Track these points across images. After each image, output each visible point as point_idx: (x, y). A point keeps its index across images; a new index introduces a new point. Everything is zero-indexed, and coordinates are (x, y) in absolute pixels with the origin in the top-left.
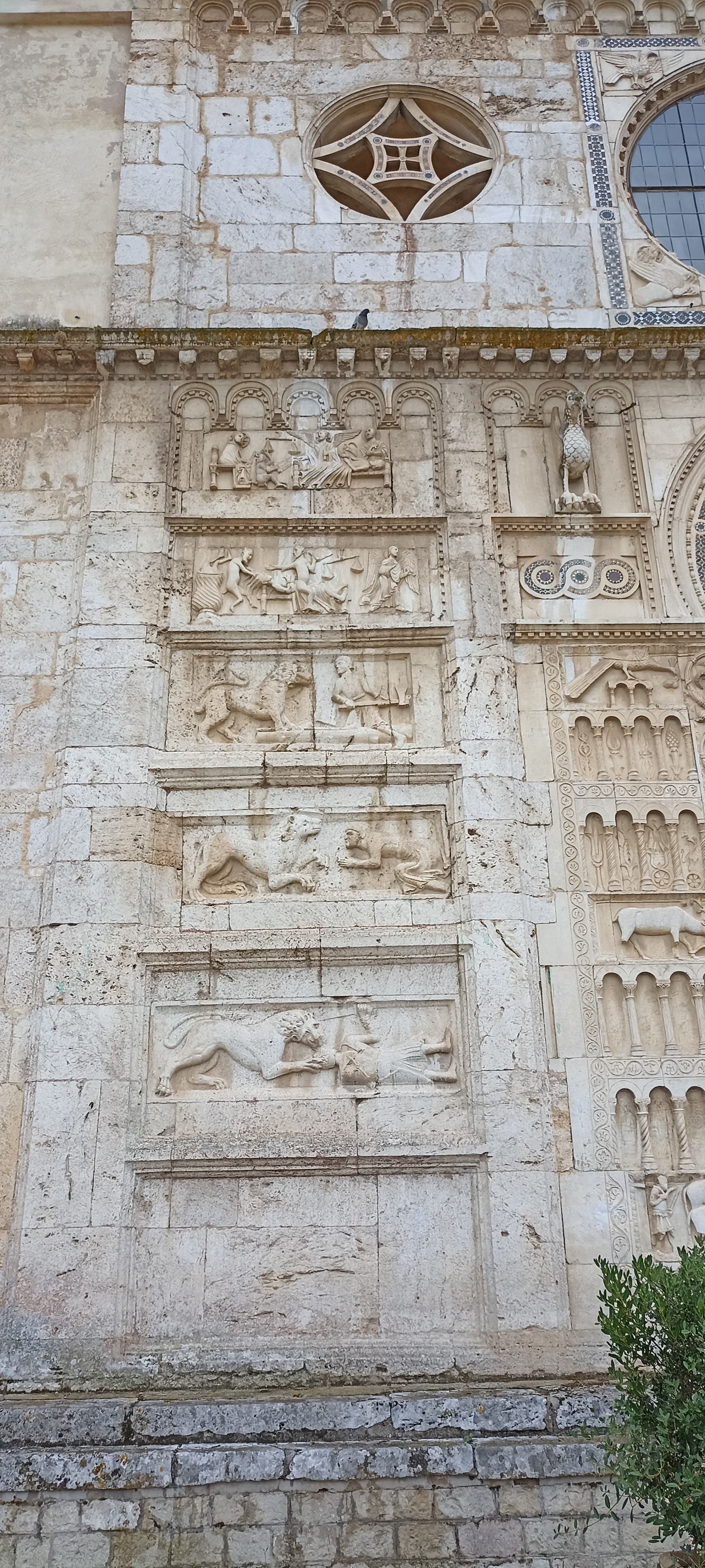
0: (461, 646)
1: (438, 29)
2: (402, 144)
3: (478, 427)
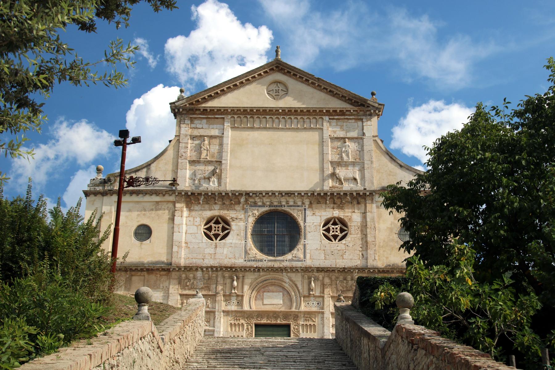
0: (216, 313)
1: (224, 204)
2: (217, 226)
3: (222, 280)
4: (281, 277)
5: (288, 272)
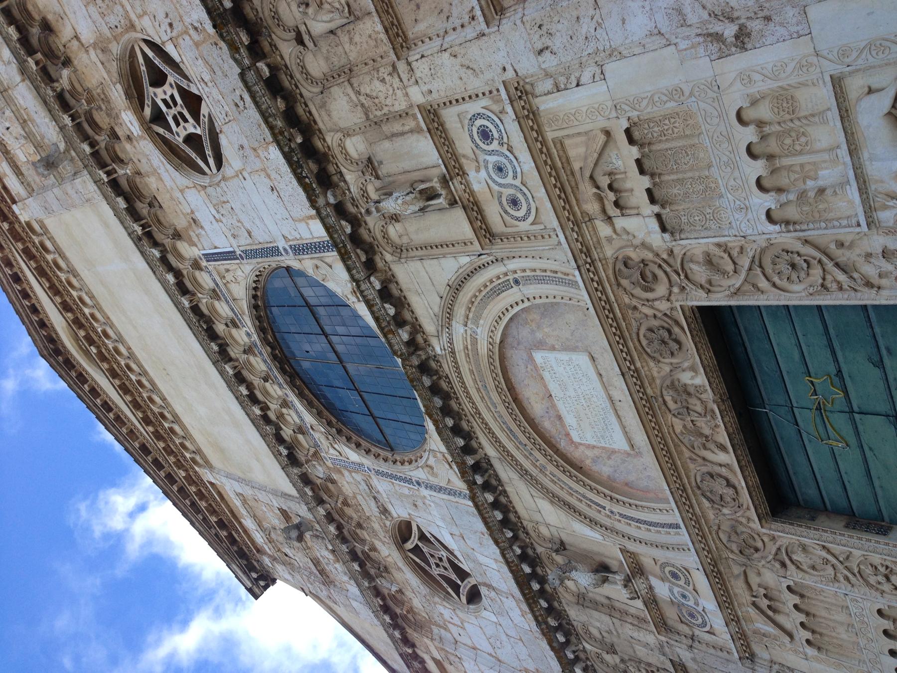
4: (461, 357)
5: (416, 328)
